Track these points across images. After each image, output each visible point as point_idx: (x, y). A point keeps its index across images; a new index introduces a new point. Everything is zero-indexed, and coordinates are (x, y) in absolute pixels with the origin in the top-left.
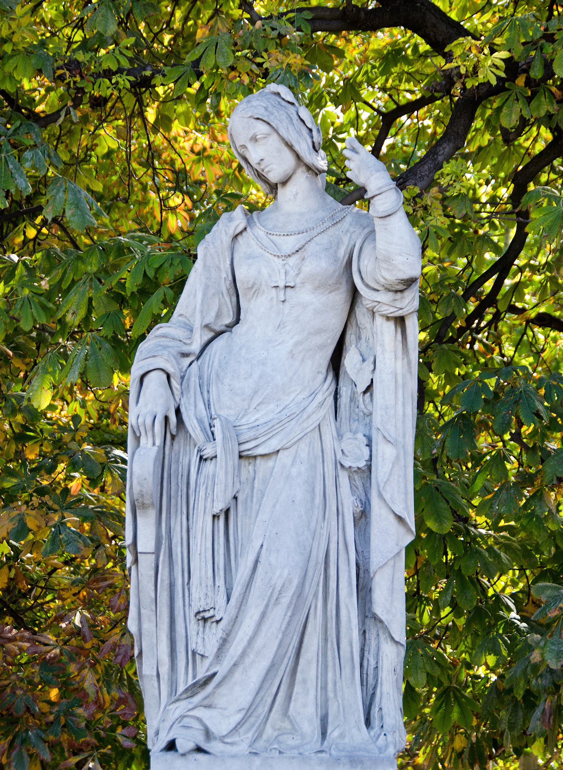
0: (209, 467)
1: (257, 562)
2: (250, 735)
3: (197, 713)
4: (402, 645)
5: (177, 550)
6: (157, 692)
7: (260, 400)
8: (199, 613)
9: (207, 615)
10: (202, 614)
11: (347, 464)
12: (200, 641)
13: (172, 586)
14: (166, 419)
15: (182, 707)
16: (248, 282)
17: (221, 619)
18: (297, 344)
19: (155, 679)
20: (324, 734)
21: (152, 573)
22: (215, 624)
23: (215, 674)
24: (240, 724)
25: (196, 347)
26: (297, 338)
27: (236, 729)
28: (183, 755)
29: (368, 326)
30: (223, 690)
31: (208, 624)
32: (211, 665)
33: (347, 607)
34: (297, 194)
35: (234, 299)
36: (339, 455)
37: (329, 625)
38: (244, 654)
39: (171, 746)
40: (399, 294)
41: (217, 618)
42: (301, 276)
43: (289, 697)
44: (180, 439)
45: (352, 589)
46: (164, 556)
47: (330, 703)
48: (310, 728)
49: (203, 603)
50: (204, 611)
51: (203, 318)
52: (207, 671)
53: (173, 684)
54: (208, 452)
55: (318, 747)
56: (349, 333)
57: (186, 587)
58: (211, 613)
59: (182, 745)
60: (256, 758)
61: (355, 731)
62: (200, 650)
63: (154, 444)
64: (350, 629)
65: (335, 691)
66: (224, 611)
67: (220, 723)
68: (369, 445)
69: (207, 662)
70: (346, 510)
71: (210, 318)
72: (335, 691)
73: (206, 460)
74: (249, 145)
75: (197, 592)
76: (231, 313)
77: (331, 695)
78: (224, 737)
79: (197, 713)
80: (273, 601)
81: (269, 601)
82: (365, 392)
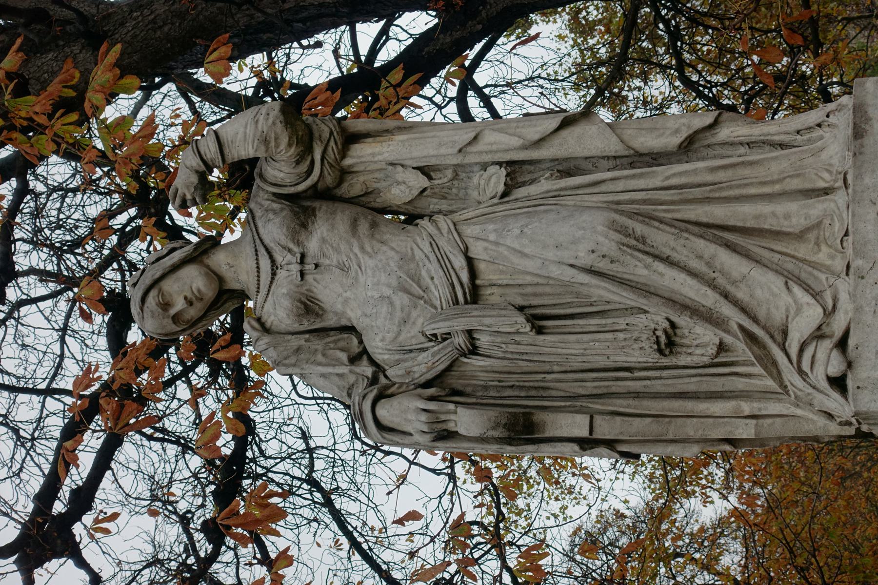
0: (483, 340)
1: (591, 271)
2: (823, 277)
3: (794, 351)
4: (720, 114)
5: (590, 387)
6: (778, 420)
7: (415, 285)
8: (660, 351)
9: (663, 339)
10: (663, 347)
11: (501, 188)
12: (699, 351)
13: (637, 395)
14: (431, 399)
15: (790, 375)
16: (298, 308)
17: (668, 319)
18: (362, 248)
19: (761, 421)
20: (826, 191)
21: (618, 419)
22: (678, 331)
23: (742, 328)
24: (807, 288)
25: (369, 371)
26: (356, 250)
27: (816, 295)
28: (850, 365)
29: (362, 179)
30: (761, 314)
31: (677, 340)
32: (728, 332)
33: (668, 178)
34: (229, 264)
35: (332, 333)
36: (496, 201)
37: (691, 197)
38: (712, 284)
39: (839, 383)
40: (316, 135)
41: (666, 324)
42: (291, 246)
43: (777, 234)
44: (455, 382)
45: (648, 173)
46: (597, 403)
47: (788, 188)
48: (817, 208)
49: (646, 345)
50: (658, 342)
51: (343, 364)
52: (739, 339)
53: (765, 394)
54: (460, 340)
55: (842, 193)
56: (373, 205)
57: (638, 374)
58: (659, 333)
59: (836, 367)
60: (853, 266)
61: (824, 156)
62: (712, 350)
63: (455, 413)
64: (695, 172)
65: (773, 182)
66: (658, 317)
67: (807, 318)
68: (484, 167)
69: (728, 339)
70: (555, 187)
71: (343, 356)
72: (773, 182)
73: (475, 347)
74: (173, 311)
75: (635, 357)
76: (346, 335)
77: (777, 188)
78: (825, 310)
79: (794, 351)
80: (641, 246)
81: (639, 250)
82: (430, 178)
